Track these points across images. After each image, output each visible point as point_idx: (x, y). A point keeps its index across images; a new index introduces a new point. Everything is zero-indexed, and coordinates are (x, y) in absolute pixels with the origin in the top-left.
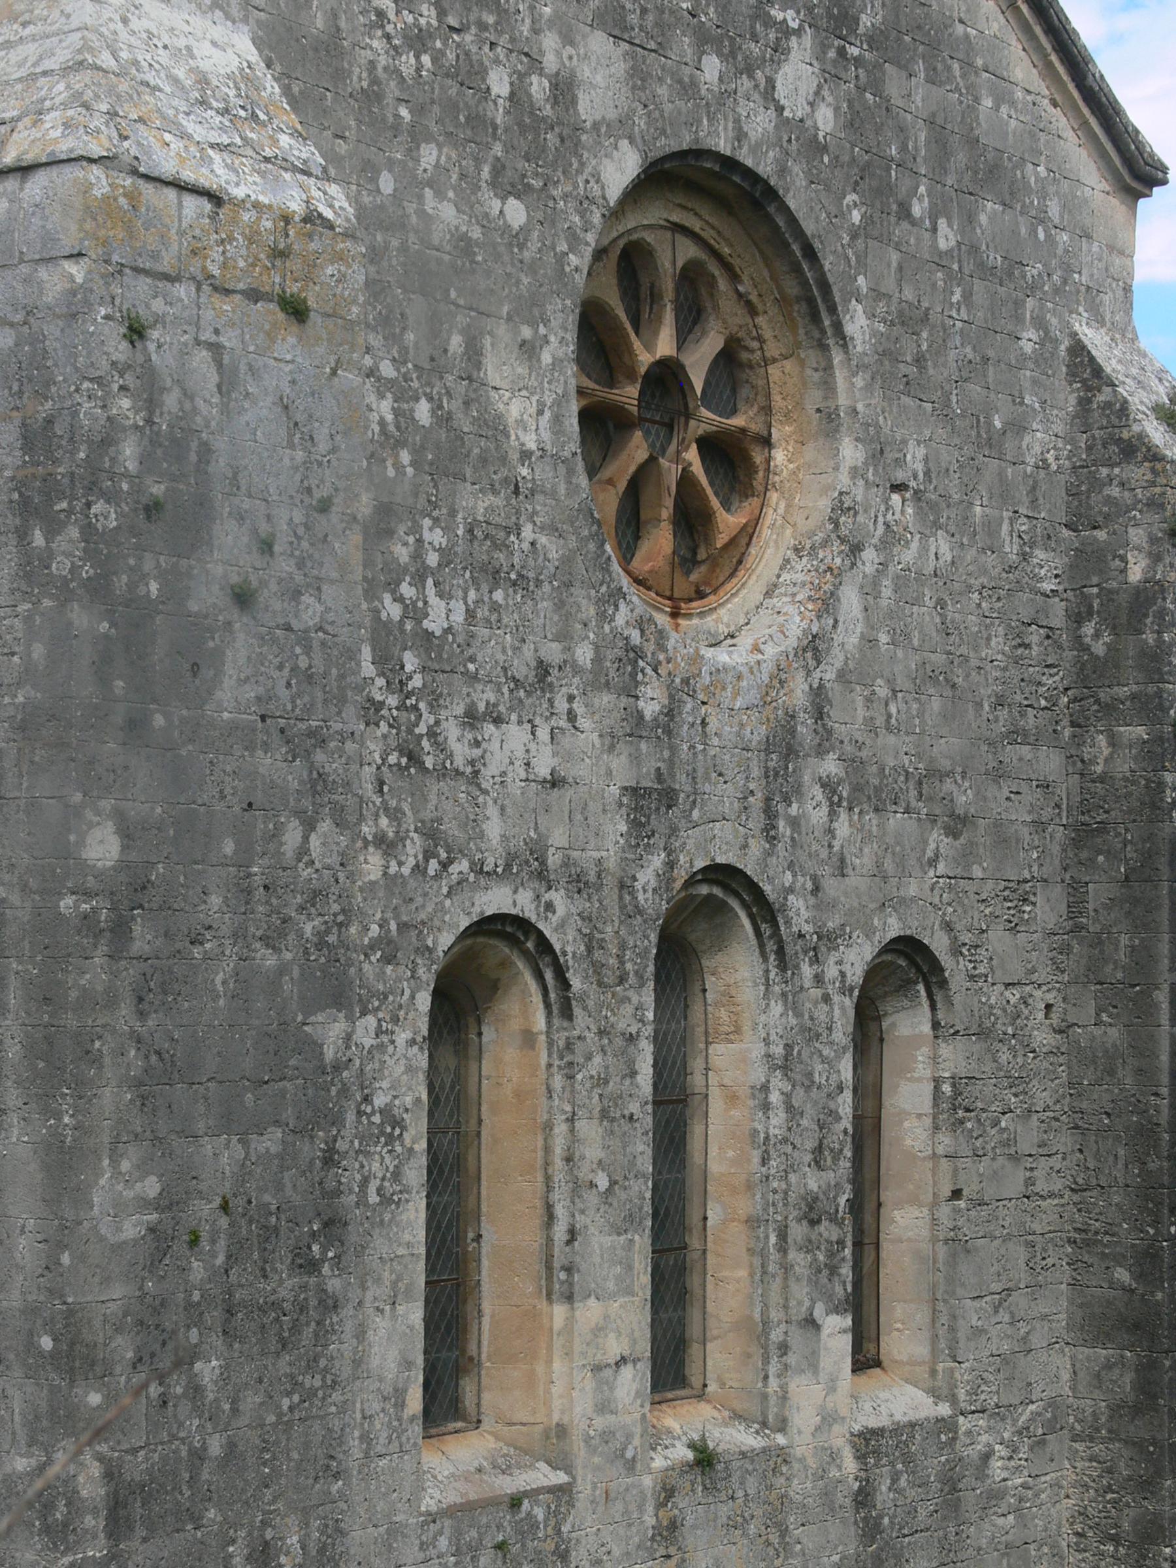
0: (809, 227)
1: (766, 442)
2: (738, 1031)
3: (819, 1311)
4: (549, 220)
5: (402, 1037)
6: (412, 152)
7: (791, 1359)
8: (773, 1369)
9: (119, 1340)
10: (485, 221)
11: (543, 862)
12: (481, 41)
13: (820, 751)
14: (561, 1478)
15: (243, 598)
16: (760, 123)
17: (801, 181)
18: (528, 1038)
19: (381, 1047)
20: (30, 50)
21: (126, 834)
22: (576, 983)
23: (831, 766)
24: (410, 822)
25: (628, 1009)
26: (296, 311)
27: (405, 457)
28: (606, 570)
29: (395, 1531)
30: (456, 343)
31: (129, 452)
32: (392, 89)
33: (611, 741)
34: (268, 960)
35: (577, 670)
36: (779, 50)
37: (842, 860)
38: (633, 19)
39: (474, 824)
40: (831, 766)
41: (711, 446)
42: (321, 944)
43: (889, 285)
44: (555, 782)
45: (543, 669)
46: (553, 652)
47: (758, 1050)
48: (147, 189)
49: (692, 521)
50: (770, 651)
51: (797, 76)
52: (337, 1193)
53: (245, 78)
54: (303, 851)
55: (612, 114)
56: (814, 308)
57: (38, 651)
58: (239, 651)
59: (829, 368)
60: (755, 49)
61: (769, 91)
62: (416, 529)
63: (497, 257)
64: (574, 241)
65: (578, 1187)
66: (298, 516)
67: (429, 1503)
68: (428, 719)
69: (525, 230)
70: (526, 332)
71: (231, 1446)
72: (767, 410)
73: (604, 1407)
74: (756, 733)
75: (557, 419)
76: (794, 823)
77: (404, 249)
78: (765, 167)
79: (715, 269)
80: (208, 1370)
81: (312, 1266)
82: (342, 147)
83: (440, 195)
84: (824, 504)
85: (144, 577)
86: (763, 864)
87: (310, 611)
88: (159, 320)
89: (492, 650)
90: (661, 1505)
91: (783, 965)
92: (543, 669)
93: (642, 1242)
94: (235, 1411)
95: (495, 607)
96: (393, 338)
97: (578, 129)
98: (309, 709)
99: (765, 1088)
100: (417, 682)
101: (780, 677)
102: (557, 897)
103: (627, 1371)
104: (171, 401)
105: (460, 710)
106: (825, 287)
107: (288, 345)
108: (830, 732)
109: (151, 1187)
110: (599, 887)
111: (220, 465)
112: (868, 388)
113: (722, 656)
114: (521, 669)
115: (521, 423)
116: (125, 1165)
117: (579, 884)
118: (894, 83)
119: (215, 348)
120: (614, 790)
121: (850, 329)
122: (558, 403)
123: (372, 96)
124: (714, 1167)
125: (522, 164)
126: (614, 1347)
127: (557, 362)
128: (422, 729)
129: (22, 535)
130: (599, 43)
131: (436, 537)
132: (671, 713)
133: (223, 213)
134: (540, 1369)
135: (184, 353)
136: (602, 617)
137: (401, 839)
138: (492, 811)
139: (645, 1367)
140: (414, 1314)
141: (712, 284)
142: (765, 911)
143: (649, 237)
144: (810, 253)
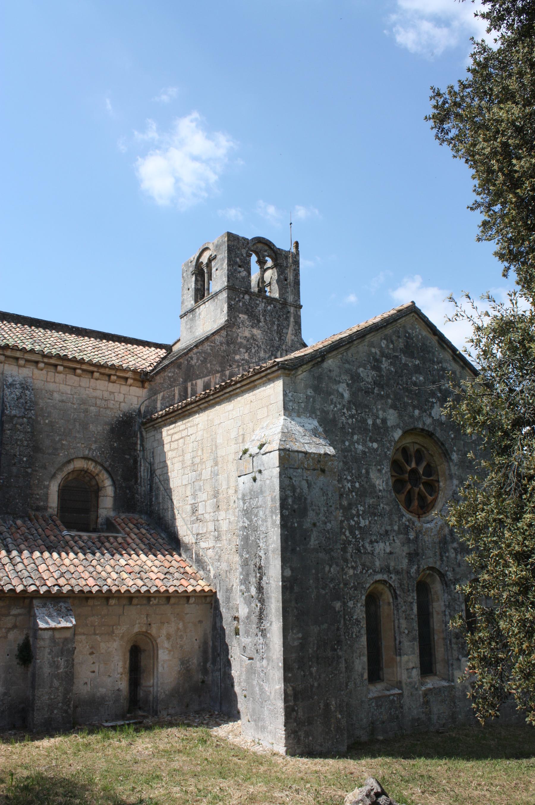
0: (442, 439)
1: (438, 481)
2: (438, 600)
3: (460, 657)
4: (383, 445)
5: (359, 605)
6: (352, 437)
7: (454, 667)
8: (450, 669)
9: (295, 664)
10: (369, 448)
11: (389, 569)
12: (365, 415)
13: (453, 542)
14: (400, 692)
15: (314, 525)
17: (439, 431)
18: (389, 604)
19: (355, 607)
20: (274, 429)
21: (292, 570)
22: (398, 592)
23: (455, 545)
24: (359, 563)
25: (410, 597)
26: (323, 471)
27: (354, 494)
28: (399, 510)
29: (362, 702)
30: (364, 471)
31: (290, 501)
32: (347, 426)
33: (403, 544)
35: (394, 531)
36: (432, 407)
37: (459, 564)
38: (399, 406)
39: (373, 563)
40: (455, 545)
41: (425, 484)
42: (334, 588)
44: (391, 553)
45: (387, 531)
46: (389, 528)
47: (443, 604)
48: (291, 453)
49: (422, 498)
50: (439, 523)
52: (340, 636)
54: (330, 571)
55: (395, 424)
56: (446, 455)
57: (275, 538)
58: (314, 535)
59: (449, 466)
60: (426, 407)
61: (430, 415)
62: (357, 507)
63: (372, 454)
65: (401, 633)
66: (325, 509)
67: (370, 696)
68: (362, 543)
69: (377, 448)
70: (379, 467)
71: (319, 685)
72: (438, 475)
73: (409, 677)
74: (437, 540)
75: (387, 483)
76: (447, 557)
77: (351, 455)
78: (431, 429)
79: (423, 449)
80: (314, 670)
81: (335, 650)
82: (337, 438)
83: (358, 444)
84: (451, 493)
85: (294, 523)
86: (441, 567)
87: (329, 526)
88: (295, 476)
89: (375, 528)
90: (424, 697)
91: (447, 586)
92: (387, 531)
94: (320, 678)
95: (375, 520)
96: (350, 472)
97: (388, 428)
98: (329, 545)
99: (445, 611)
100: (359, 536)
102: (393, 576)
103: (415, 670)
104: (298, 490)
105: (368, 541)
106: (446, 450)
107: (322, 478)
108: (454, 538)
109: (300, 635)
110: (402, 573)
111: (309, 501)
112: (458, 469)
113: (428, 525)
115: (379, 485)
116: (294, 631)
117: (397, 573)
119: (307, 481)
120: (405, 554)
121: (453, 458)
122: (387, 480)
123: (343, 428)
124: (435, 628)
125: (376, 436)
126: (411, 665)
127: (386, 472)
128: (360, 545)
129: (272, 516)
130: (391, 411)
131: (362, 508)
132: (417, 537)
133: (307, 456)
134: (395, 669)
135: (300, 481)
136: (399, 520)
137: (357, 566)
138: (377, 560)
139: (419, 669)
140: (365, 659)
141: (423, 452)
142: (442, 576)
143: (408, 445)
144: (442, 444)
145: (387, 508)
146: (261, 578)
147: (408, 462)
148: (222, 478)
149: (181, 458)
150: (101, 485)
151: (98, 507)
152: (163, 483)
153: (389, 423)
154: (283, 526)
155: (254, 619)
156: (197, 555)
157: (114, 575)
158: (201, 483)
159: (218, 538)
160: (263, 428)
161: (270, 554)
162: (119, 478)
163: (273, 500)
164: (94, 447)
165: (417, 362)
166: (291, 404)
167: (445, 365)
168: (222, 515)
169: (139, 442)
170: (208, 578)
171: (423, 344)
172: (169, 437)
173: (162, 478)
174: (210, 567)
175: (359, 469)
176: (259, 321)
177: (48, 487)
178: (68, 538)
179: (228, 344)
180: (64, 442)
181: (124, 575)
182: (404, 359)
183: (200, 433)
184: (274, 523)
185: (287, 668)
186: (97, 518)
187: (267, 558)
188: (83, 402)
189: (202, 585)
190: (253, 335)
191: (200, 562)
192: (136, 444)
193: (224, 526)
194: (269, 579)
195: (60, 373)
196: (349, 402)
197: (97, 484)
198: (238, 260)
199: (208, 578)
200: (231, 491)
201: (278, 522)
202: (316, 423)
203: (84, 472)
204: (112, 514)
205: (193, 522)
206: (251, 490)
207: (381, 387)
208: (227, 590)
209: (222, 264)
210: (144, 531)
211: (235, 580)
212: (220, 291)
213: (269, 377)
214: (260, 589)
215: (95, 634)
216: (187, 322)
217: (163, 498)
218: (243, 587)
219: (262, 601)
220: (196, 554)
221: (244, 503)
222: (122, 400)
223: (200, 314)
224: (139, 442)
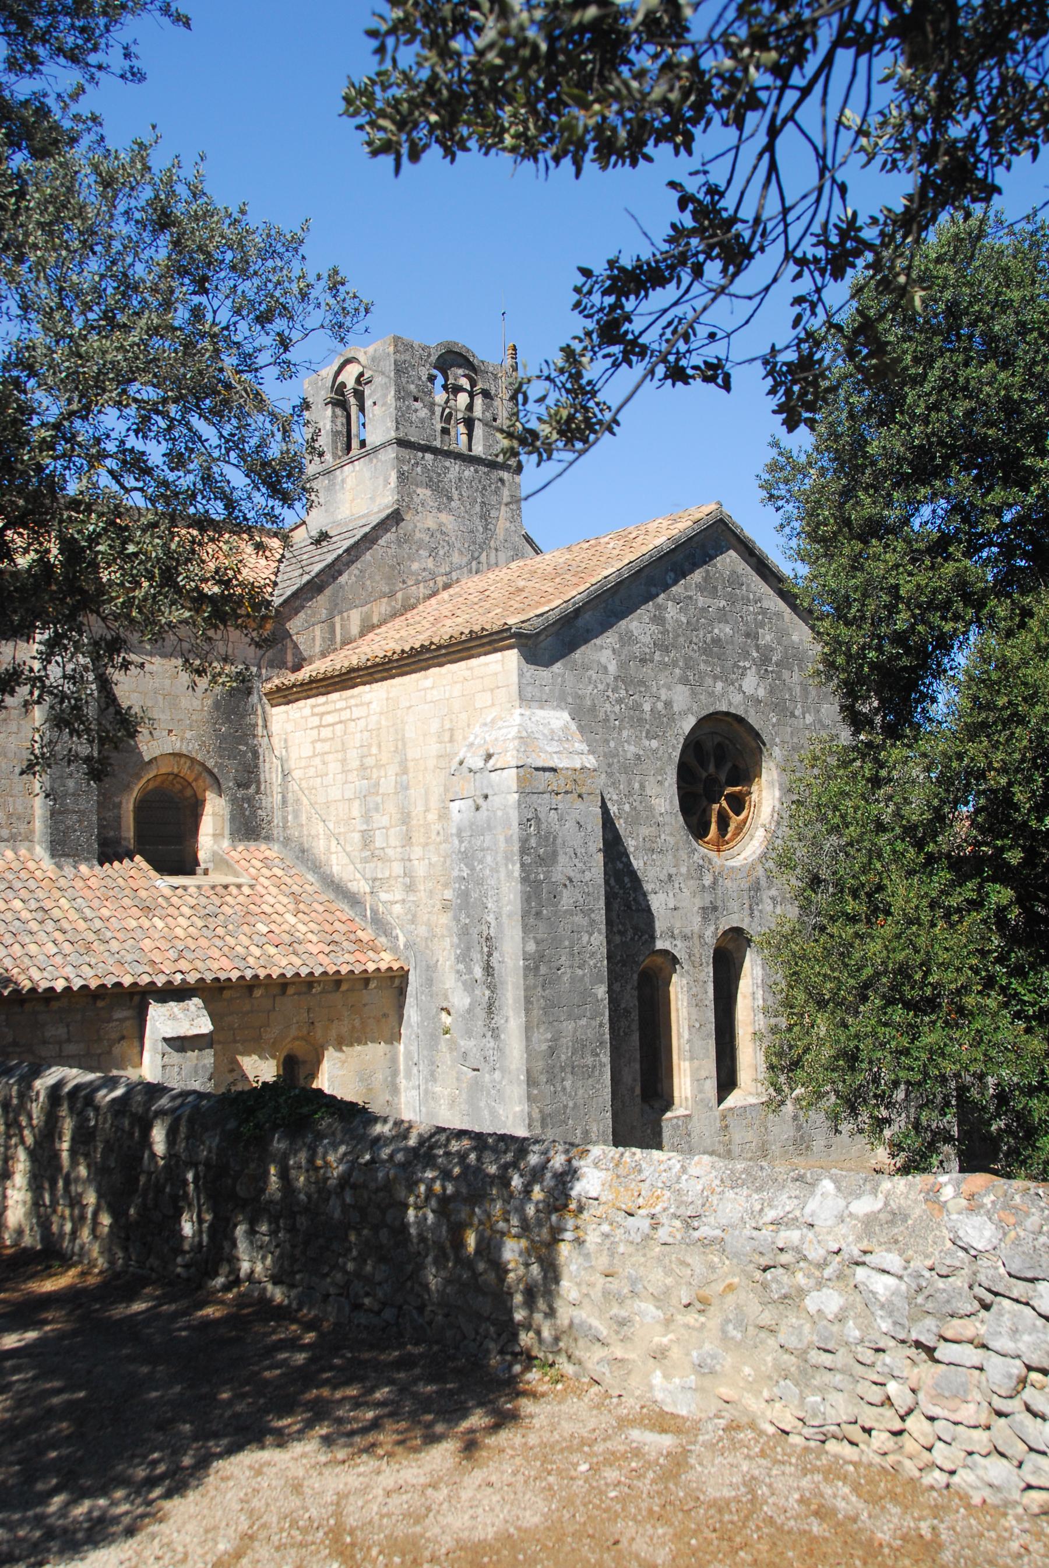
16: (737, 698)
21: (537, 943)
23: (773, 892)
30: (637, 786)
31: (533, 842)
32: (612, 717)
34: (580, 972)
40: (773, 892)
41: (730, 798)
43: (788, 738)
45: (670, 876)
46: (673, 871)
51: (750, 683)
53: (566, 728)
64: (674, 747)
74: (745, 885)
78: (740, 712)
80: (568, 1084)
92: (670, 876)
93: (712, 1042)
101: (753, 867)
102: (678, 942)
111: (559, 841)
114: (663, 876)
117: (685, 938)
118: (786, 674)
123: (606, 720)
126: (704, 1074)
130: (680, 688)
132: (715, 882)
140: (637, 1066)
145: (671, 840)
146: (490, 955)
147: (703, 764)
148: (415, 793)
149: (340, 756)
153: (676, 708)
154: (525, 880)
155: (481, 1013)
156: (374, 912)
157: (257, 952)
158: (379, 799)
159: (410, 888)
161: (504, 919)
163: (508, 840)
164: (188, 735)
165: (723, 603)
166: (529, 688)
167: (765, 604)
168: (417, 852)
169: (260, 722)
170: (394, 949)
171: (734, 572)
172: (317, 719)
173: (304, 785)
175: (629, 783)
176: (450, 499)
177: (119, 806)
178: (168, 892)
179: (399, 542)
181: (272, 950)
182: (701, 601)
183: (374, 719)
184: (509, 874)
185: (531, 1081)
187: (500, 925)
189: (386, 960)
190: (440, 525)
191: (379, 923)
192: (256, 725)
193: (420, 869)
194: (502, 955)
196: (616, 678)
197: (195, 795)
198: (412, 387)
199: (394, 949)
200: (432, 816)
201: (517, 874)
202: (566, 716)
205: (364, 860)
206: (472, 824)
207: (666, 650)
208: (428, 967)
209: (385, 396)
210: (279, 872)
211: (445, 954)
212: (383, 446)
214: (488, 969)
215: (235, 1041)
217: (309, 819)
218: (461, 967)
219: (492, 987)
221: (461, 842)
223: (343, 481)
224: (260, 722)
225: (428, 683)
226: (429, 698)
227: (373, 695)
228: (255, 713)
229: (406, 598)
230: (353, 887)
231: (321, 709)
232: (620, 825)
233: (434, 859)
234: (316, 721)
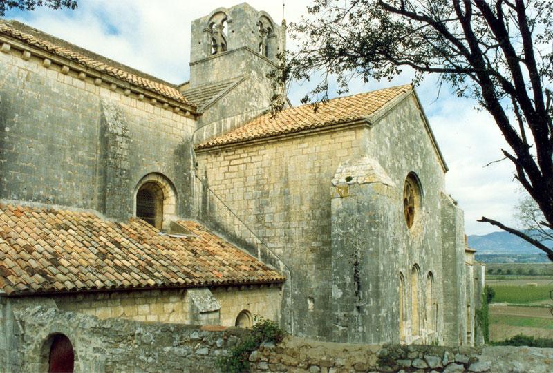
129: (370, 229)
149: (242, 179)
150: (165, 195)
151: (163, 213)
152: (219, 196)
160: (345, 164)
162: (180, 190)
164: (164, 164)
168: (294, 224)
173: (217, 193)
174: (279, 261)
180: (144, 159)
183: (267, 162)
186: (162, 220)
188: (156, 127)
195: (140, 100)
197: (163, 194)
200: (305, 207)
203: (155, 183)
204: (175, 219)
205: (258, 228)
213: (352, 127)
216: (197, 69)
220: (261, 251)
222: (181, 128)
223: (213, 65)
225: (305, 145)
226: (305, 152)
227: (268, 153)
228: (190, 158)
229: (247, 117)
230: (250, 241)
231: (231, 157)
232: (404, 217)
233: (306, 228)
234: (227, 163)
